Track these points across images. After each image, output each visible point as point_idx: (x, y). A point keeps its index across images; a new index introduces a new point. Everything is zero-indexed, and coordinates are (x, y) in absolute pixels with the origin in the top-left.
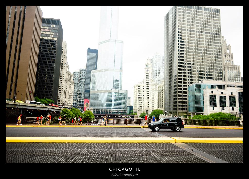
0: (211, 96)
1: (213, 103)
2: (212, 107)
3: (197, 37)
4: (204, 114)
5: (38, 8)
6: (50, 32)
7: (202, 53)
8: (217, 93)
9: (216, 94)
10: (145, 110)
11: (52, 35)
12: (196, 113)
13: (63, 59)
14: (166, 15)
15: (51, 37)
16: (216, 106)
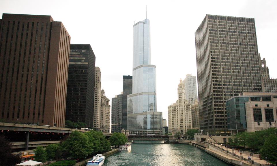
0: (254, 110)
1: (258, 118)
2: (257, 123)
3: (231, 50)
4: (247, 131)
5: (63, 29)
6: (82, 57)
7: (237, 66)
8: (262, 105)
9: (261, 107)
10: (180, 130)
11: (83, 60)
12: (237, 131)
13: (97, 84)
14: (200, 25)
15: (83, 62)
16: (262, 121)
